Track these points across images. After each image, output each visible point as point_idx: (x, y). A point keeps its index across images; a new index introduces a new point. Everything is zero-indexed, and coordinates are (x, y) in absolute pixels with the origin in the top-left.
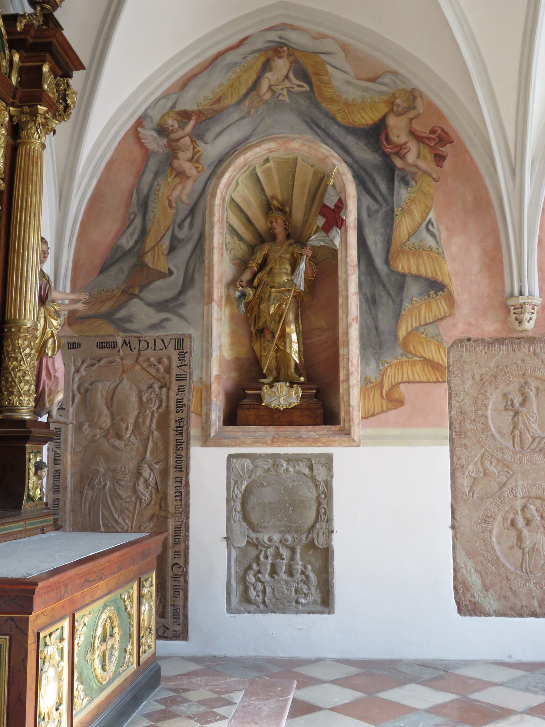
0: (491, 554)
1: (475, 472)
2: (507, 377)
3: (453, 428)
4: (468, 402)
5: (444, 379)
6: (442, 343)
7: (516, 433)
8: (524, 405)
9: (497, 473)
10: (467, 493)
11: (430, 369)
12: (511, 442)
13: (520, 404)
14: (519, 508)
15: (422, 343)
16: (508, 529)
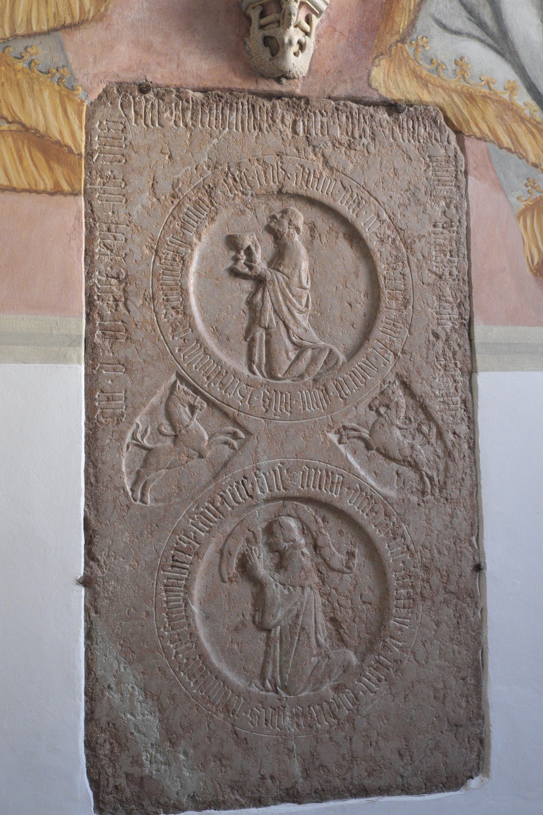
0: (189, 648)
1: (151, 433)
2: (240, 194)
3: (96, 316)
4: (136, 250)
5: (77, 186)
6: (73, 89)
7: (258, 335)
8: (280, 265)
9: (206, 437)
10: (128, 488)
11: (39, 157)
12: (244, 359)
13: (269, 265)
14: (259, 528)
15: (18, 84)
16: (231, 580)
